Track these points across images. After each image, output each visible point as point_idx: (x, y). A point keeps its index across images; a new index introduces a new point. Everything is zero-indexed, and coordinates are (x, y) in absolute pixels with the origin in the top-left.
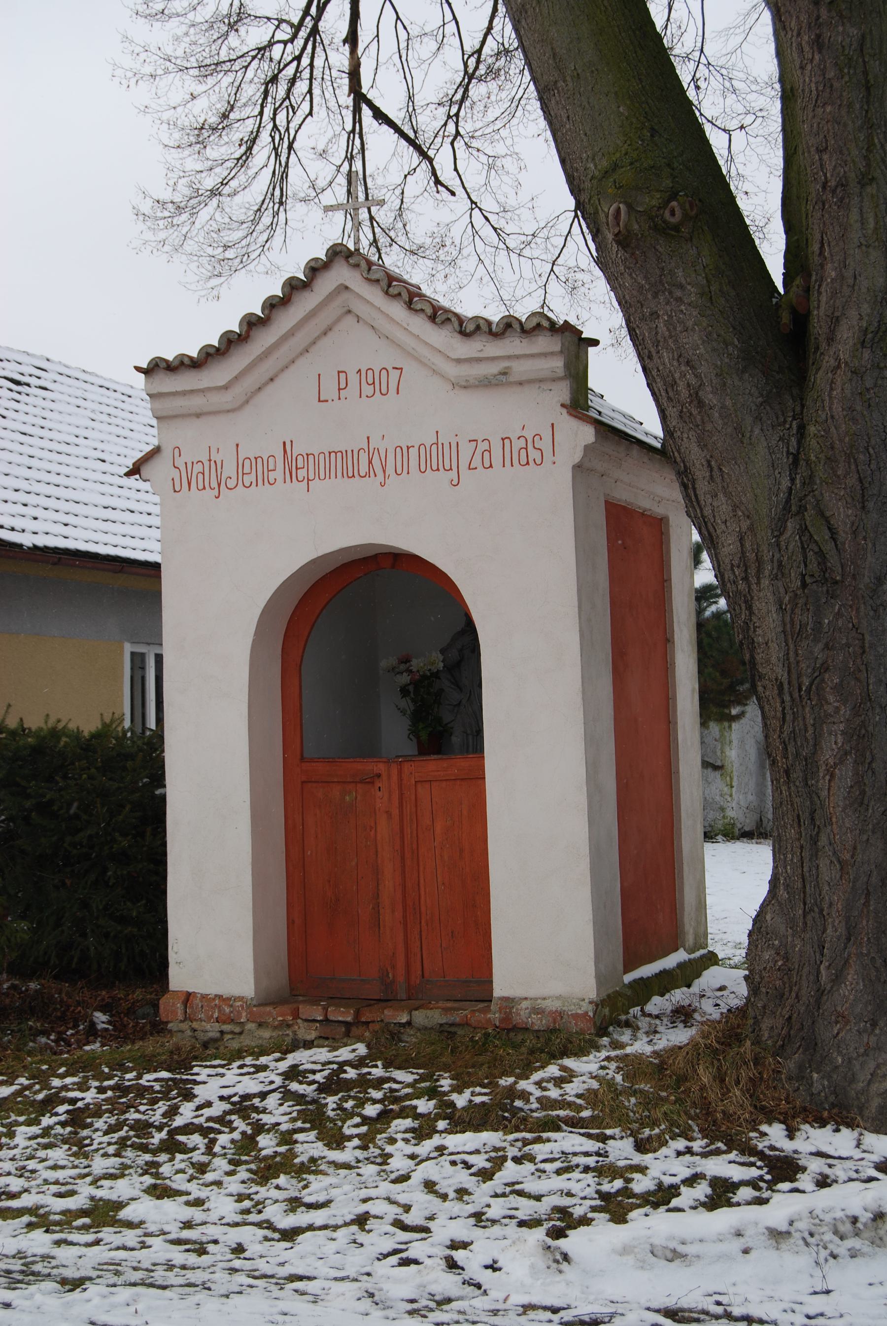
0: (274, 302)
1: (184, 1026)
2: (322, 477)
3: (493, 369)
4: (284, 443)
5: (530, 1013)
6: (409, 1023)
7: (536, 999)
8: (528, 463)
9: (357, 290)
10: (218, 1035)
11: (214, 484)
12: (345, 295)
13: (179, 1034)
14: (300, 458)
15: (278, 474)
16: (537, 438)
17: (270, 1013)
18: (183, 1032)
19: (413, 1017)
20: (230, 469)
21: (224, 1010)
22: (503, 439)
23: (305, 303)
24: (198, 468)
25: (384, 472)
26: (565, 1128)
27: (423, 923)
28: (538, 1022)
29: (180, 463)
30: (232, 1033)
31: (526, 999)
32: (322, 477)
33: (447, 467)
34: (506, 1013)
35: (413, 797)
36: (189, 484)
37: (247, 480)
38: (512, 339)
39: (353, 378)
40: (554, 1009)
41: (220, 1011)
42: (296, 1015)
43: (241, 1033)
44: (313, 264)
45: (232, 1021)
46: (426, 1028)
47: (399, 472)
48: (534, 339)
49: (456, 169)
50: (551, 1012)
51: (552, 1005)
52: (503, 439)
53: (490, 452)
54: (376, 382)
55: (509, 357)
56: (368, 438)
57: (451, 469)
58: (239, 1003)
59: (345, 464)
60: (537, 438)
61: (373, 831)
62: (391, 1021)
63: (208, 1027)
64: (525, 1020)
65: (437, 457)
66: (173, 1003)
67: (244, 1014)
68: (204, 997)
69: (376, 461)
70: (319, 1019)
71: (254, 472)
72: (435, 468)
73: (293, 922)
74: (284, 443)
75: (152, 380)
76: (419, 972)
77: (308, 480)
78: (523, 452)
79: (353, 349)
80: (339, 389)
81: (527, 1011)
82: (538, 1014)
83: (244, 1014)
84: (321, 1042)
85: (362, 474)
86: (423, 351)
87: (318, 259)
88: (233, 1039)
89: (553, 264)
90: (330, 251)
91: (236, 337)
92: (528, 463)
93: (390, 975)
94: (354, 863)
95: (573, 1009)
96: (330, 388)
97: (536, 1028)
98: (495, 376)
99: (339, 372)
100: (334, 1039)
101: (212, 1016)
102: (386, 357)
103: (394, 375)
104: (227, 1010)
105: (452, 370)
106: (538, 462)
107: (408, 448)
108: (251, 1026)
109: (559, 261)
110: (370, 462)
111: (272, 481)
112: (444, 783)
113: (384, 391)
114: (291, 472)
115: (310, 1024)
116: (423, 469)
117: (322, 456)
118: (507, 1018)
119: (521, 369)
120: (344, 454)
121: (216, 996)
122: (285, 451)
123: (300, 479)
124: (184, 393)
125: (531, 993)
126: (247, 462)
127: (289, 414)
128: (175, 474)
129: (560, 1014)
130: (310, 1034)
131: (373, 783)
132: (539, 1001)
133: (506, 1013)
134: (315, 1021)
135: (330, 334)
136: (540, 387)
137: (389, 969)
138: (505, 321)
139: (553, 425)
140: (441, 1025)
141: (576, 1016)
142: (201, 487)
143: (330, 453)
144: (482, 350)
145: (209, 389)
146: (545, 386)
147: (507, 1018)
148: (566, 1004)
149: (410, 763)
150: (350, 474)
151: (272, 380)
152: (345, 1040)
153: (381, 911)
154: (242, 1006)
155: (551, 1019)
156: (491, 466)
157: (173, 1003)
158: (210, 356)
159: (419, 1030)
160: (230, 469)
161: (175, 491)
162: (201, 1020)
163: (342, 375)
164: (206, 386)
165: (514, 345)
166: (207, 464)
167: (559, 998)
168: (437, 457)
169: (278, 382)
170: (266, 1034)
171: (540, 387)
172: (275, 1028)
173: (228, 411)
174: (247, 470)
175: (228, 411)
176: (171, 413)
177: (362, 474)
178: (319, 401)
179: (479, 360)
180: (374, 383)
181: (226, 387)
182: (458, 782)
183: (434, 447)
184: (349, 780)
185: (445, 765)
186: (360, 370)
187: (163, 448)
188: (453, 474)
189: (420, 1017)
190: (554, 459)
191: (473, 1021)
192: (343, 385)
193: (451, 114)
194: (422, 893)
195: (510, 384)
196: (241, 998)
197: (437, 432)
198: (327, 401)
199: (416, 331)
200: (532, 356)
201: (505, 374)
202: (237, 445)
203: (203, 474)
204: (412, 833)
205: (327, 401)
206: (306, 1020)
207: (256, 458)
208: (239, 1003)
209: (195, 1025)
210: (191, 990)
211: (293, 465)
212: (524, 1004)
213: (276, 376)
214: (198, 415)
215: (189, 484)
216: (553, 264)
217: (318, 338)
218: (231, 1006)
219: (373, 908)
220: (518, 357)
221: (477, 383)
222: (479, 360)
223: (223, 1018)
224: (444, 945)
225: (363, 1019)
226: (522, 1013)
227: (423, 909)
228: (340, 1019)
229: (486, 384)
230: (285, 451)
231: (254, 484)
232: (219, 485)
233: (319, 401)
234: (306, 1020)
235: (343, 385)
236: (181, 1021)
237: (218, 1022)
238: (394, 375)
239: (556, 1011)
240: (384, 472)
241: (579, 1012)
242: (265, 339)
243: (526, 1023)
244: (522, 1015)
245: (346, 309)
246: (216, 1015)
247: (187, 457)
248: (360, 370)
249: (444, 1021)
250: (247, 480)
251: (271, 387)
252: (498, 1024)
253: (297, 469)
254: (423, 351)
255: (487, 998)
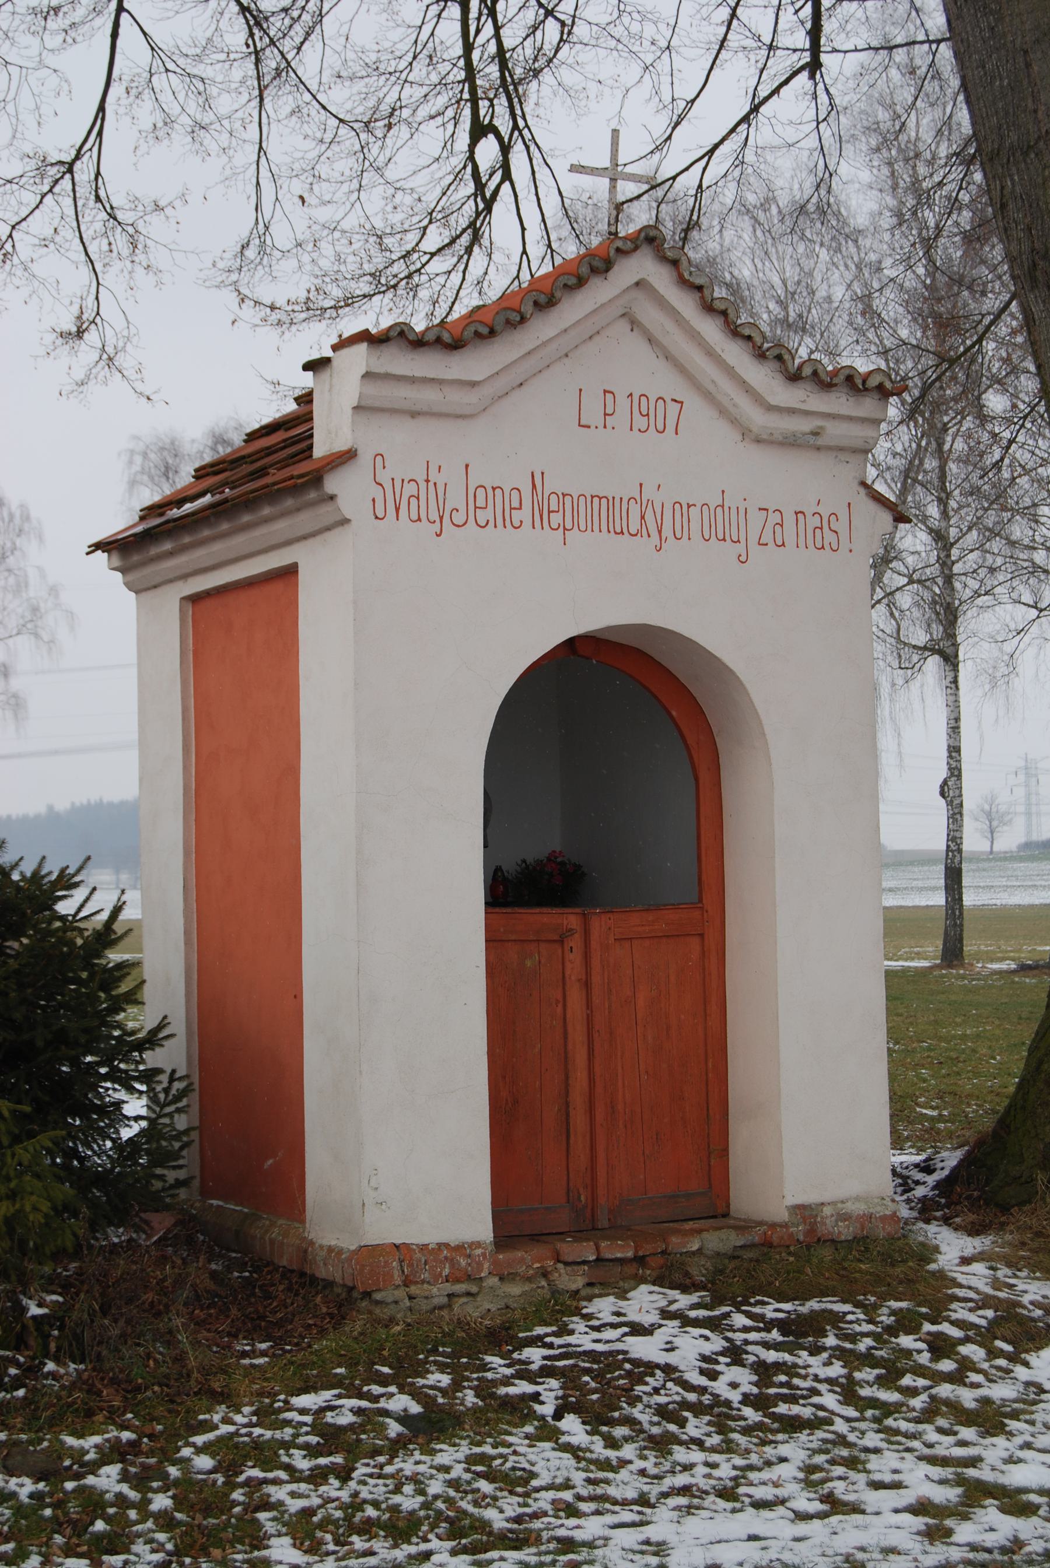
3: (804, 425)
10: (446, 1299)
11: (434, 516)
17: (522, 1260)
20: (456, 498)
21: (459, 1263)
24: (410, 489)
25: (660, 532)
28: (845, 1231)
29: (384, 477)
30: (469, 1294)
32: (583, 528)
36: (397, 510)
39: (623, 403)
41: (452, 1266)
45: (469, 1278)
50: (859, 1217)
51: (857, 1208)
54: (648, 414)
58: (479, 1251)
59: (608, 513)
60: (833, 517)
61: (560, 1005)
63: (435, 1290)
65: (721, 524)
66: (386, 1262)
67: (486, 1265)
68: (423, 1248)
69: (649, 516)
71: (491, 507)
72: (721, 537)
83: (486, 1265)
84: (589, 1291)
85: (633, 531)
86: (726, 387)
89: (13, 227)
93: (583, 1198)
94: (537, 1050)
96: (593, 413)
97: (843, 1238)
98: (804, 434)
99: (605, 392)
101: (440, 1274)
102: (663, 382)
104: (463, 1262)
105: (758, 419)
107: (689, 506)
108: (494, 1281)
110: (643, 517)
111: (516, 524)
113: (660, 427)
114: (542, 514)
115: (576, 1268)
117: (582, 499)
119: (836, 432)
120: (610, 501)
122: (534, 486)
124: (412, 380)
125: (826, 1197)
130: (575, 1281)
132: (840, 1205)
134: (584, 1262)
135: (596, 339)
137: (581, 1190)
146: (843, 457)
147: (811, 1231)
154: (484, 1255)
156: (783, 545)
160: (456, 498)
162: (423, 1282)
166: (423, 485)
167: (858, 1199)
168: (721, 524)
172: (529, 1279)
174: (480, 502)
176: (377, 404)
181: (771, 408)
184: (531, 937)
200: (850, 419)
206: (566, 1264)
208: (479, 1251)
209: (413, 1289)
210: (398, 1242)
211: (549, 508)
214: (414, 414)
215: (397, 510)
218: (469, 1256)
222: (792, 411)
228: (619, 1255)
229: (790, 442)
230: (534, 486)
232: (441, 518)
240: (660, 532)
241: (888, 1213)
246: (446, 1271)
252: (801, 1238)
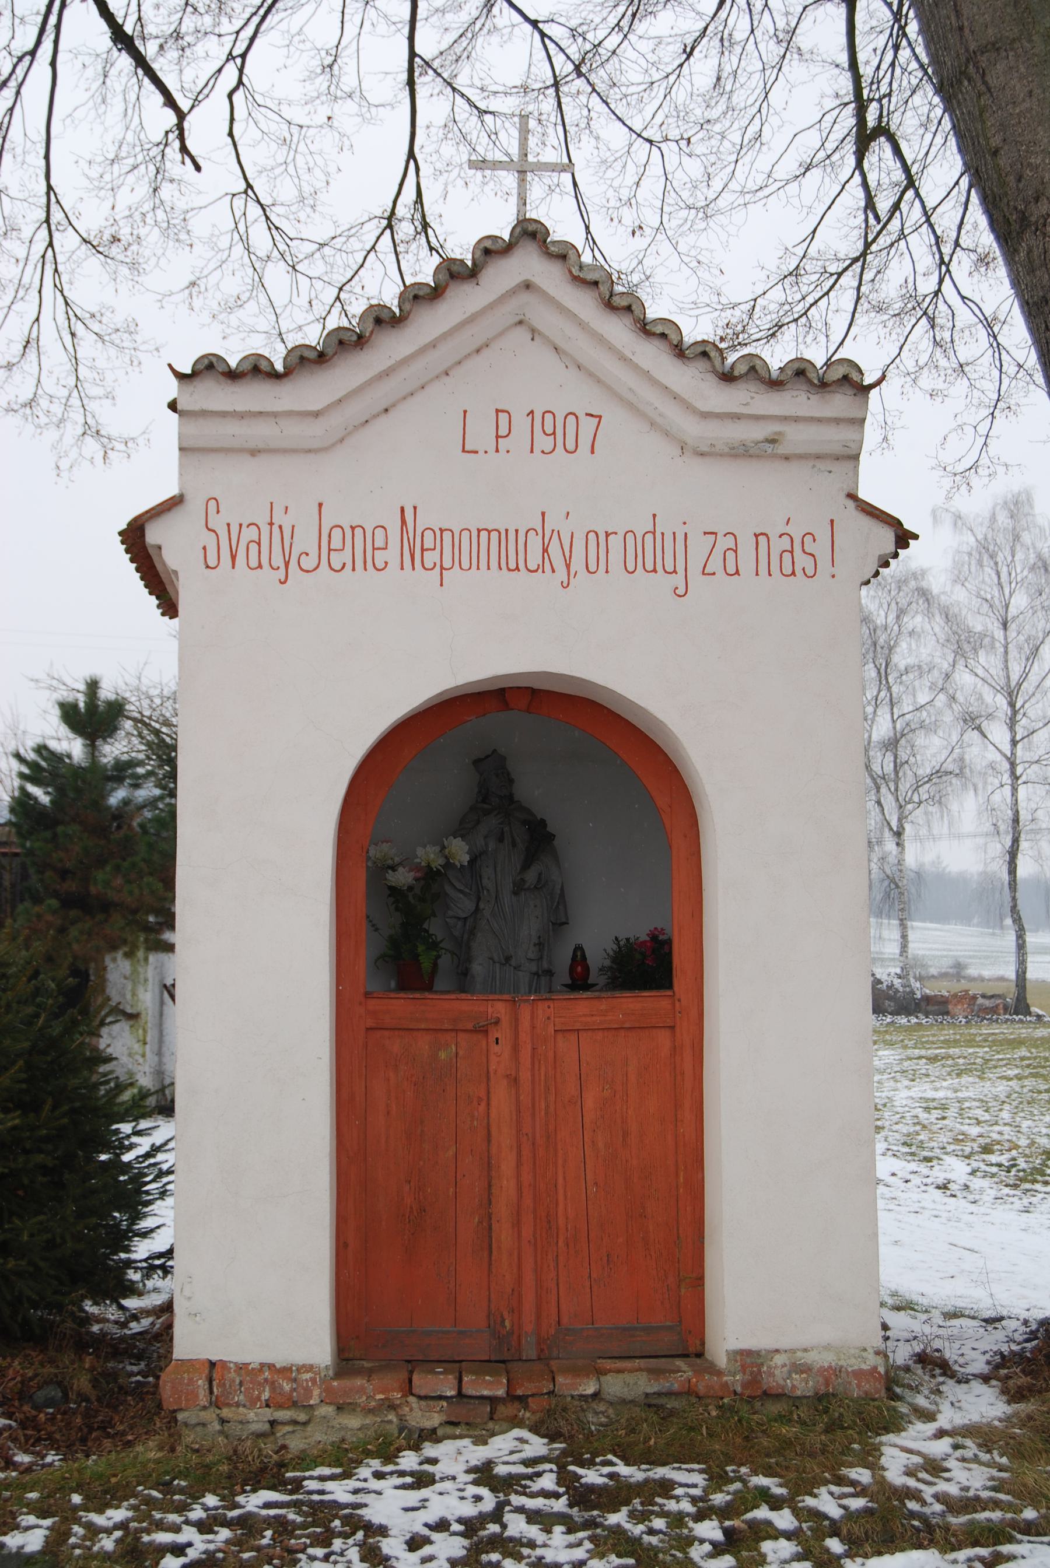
0: (421, 293)
1: (210, 1415)
2: (465, 564)
3: (757, 432)
4: (402, 510)
5: (790, 1373)
6: (596, 1395)
7: (793, 1351)
8: (793, 573)
9: (552, 291)
10: (267, 1426)
11: (278, 561)
12: (525, 297)
13: (199, 1429)
14: (428, 533)
15: (392, 554)
16: (808, 538)
17: (362, 1390)
18: (204, 1425)
19: (604, 1386)
20: (306, 541)
21: (281, 1387)
22: (756, 536)
23: (463, 301)
24: (250, 534)
25: (568, 566)
26: (1019, 1536)
27: (561, 1244)
28: (802, 1386)
29: (218, 522)
30: (295, 1422)
31: (777, 1351)
32: (465, 564)
33: (670, 569)
34: (752, 1373)
35: (551, 1054)
36: (233, 558)
37: (337, 560)
38: (795, 393)
39: (522, 424)
40: (826, 1365)
41: (273, 1389)
42: (409, 1390)
43: (305, 1424)
44: (488, 244)
45: (294, 1405)
46: (624, 1402)
47: (592, 568)
48: (828, 396)
49: (231, 134)
50: (822, 1370)
51: (823, 1359)
52: (756, 536)
53: (736, 552)
54: (555, 432)
55: (785, 419)
56: (543, 514)
57: (675, 571)
58: (308, 1376)
59: (502, 549)
60: (808, 538)
61: (483, 1104)
62: (566, 1393)
63: (251, 1415)
64: (782, 1382)
65: (652, 552)
66: (190, 1380)
67: (316, 1392)
68: (241, 1368)
69: (554, 549)
70: (449, 1394)
71: (350, 548)
72: (650, 567)
73: (346, 1245)
74: (402, 510)
75: (191, 388)
76: (555, 1317)
77: (442, 568)
78: (787, 557)
79: (529, 379)
80: (497, 437)
81: (785, 1369)
82: (802, 1372)
83: (316, 1392)
84: (449, 1430)
85: (532, 566)
86: (647, 394)
87: (496, 237)
88: (293, 1432)
89: (341, 289)
90: (518, 230)
91: (355, 338)
92: (793, 573)
93: (507, 1323)
94: (451, 1153)
95: (855, 1364)
96: (481, 434)
97: (799, 1393)
98: (757, 443)
99: (497, 411)
100: (467, 1424)
101: (259, 1398)
102: (572, 395)
103: (588, 426)
104: (287, 1387)
105: (692, 429)
106: (810, 573)
107: (607, 535)
108: (328, 1410)
109: (347, 288)
110: (545, 550)
111: (380, 564)
112: (600, 1035)
113: (571, 446)
114: (413, 553)
115: (431, 1403)
116: (631, 568)
117: (466, 534)
118: (754, 1380)
119: (797, 438)
120: (503, 535)
121: (262, 1365)
122: (404, 522)
123: (429, 564)
124: (241, 416)
125: (784, 1343)
126: (337, 534)
127: (409, 462)
128: (210, 541)
129: (837, 1371)
130: (430, 1418)
131: (486, 1032)
132: (799, 1354)
133: (752, 1373)
134: (441, 1398)
135: (485, 352)
136: (814, 466)
137: (506, 1314)
138: (796, 365)
139: (832, 521)
140: (647, 1395)
141: (859, 1374)
142: (254, 563)
143: (479, 531)
144: (747, 404)
145: (290, 414)
146: (821, 465)
147: (754, 1380)
148: (842, 1356)
149: (546, 1003)
150: (512, 566)
151: (386, 410)
152: (491, 1425)
153: (495, 1226)
154: (313, 1380)
155: (821, 1379)
156: (737, 573)
157: (190, 1380)
158: (306, 360)
159: (611, 1404)
160: (306, 541)
161: (208, 567)
162: (238, 1405)
163: (503, 417)
164: (286, 408)
165: (797, 401)
166: (265, 530)
167: (827, 1348)
168: (652, 552)
169: (392, 413)
170: (353, 1422)
171: (814, 466)
172: (371, 1411)
173: (310, 451)
174: (336, 543)
175: (310, 451)
177: (532, 566)
178: (464, 451)
179: (736, 417)
180: (554, 433)
182: (622, 1033)
183: (649, 538)
184: (446, 1026)
185: (603, 1007)
186: (532, 412)
187: (188, 497)
188: (678, 580)
189: (615, 1386)
190: (834, 571)
191: (701, 1389)
192: (503, 431)
193: (234, 54)
194: (561, 1197)
195: (775, 456)
196: (309, 1368)
197: (654, 516)
198: (477, 452)
199: (645, 365)
200: (819, 420)
201: (773, 441)
202: (320, 505)
203: (259, 544)
204: (547, 1107)
205: (477, 452)
206: (420, 1398)
207: (353, 528)
208: (308, 1376)
209: (226, 1413)
210: (214, 1358)
211: (417, 544)
212: (779, 1360)
213: (394, 405)
214: (254, 452)
215: (233, 558)
216: (341, 289)
217: (468, 356)
218: (295, 1380)
219: (480, 1222)
220: (796, 419)
221: (727, 450)
222: (736, 417)
223: (279, 1399)
224: (594, 1275)
225: (519, 1392)
226: (777, 1372)
227: (561, 1221)
228: (486, 1393)
229: (741, 452)
230: (404, 522)
231: (349, 566)
232: (287, 564)
233: (464, 451)
234: (426, 1398)
235: (503, 431)
236: (205, 1408)
237: (268, 1406)
238: (588, 426)
239: (830, 1367)
240: (568, 566)
241: (864, 1367)
242: (392, 347)
243: (783, 1388)
244: (778, 1374)
245: (518, 319)
246: (266, 1395)
247: (231, 514)
248: (532, 412)
249: (655, 1389)
250: (337, 560)
251: (384, 419)
252: (739, 1389)
253: (423, 550)
254: (647, 394)
255: (694, 1351)
